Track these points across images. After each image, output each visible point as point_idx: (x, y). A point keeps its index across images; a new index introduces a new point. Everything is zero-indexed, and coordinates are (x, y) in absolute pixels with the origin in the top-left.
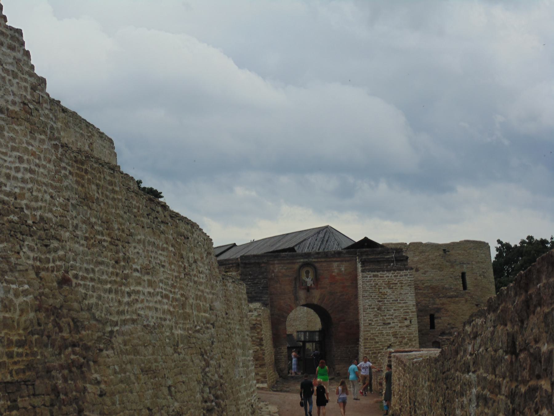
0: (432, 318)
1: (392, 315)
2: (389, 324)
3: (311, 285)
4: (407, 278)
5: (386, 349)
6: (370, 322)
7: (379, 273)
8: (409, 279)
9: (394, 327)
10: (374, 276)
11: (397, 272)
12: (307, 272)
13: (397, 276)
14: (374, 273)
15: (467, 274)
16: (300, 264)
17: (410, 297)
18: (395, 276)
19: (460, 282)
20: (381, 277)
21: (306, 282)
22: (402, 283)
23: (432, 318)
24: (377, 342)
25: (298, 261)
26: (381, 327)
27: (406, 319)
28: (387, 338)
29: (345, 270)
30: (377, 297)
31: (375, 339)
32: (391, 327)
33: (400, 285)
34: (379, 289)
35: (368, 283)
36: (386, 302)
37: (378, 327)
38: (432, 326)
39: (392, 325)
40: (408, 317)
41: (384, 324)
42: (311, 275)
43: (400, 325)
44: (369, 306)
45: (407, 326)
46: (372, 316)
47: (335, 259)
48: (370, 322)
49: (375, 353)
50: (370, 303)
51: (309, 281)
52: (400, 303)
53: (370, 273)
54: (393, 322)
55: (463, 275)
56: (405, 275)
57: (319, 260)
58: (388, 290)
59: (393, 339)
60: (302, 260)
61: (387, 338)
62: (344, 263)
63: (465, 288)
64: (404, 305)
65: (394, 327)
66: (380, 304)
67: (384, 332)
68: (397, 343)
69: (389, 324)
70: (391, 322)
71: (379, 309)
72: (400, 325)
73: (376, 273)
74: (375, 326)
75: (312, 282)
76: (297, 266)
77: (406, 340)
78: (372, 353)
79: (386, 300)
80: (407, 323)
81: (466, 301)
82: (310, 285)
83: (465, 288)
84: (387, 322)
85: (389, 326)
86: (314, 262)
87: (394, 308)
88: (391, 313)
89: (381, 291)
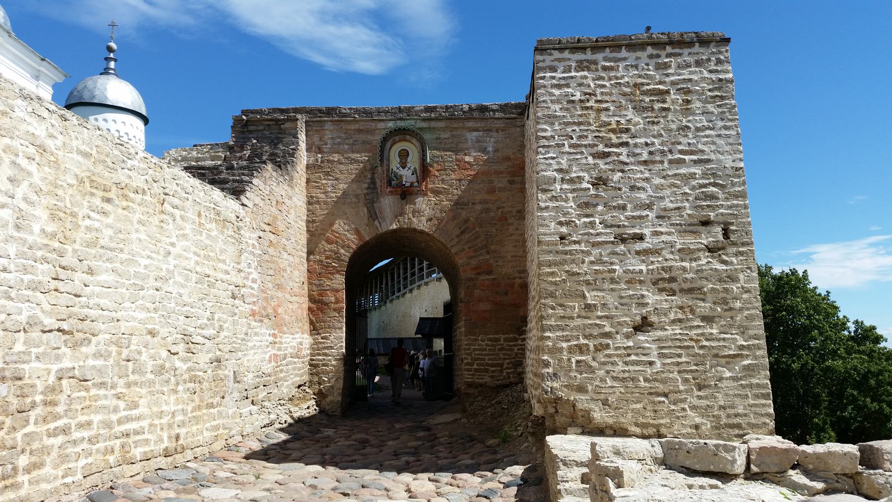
1: (649, 207)
2: (641, 238)
3: (412, 184)
4: (706, 74)
5: (628, 336)
6: (564, 230)
8: (714, 77)
9: (657, 252)
10: (581, 66)
11: (669, 49)
12: (404, 155)
13: (667, 66)
14: (580, 56)
16: (384, 132)
17: (720, 142)
20: (605, 69)
21: (399, 178)
22: (688, 92)
25: (381, 125)
26: (605, 251)
27: (706, 223)
29: (496, 151)
30: (589, 141)
31: (584, 297)
32: (646, 252)
33: (680, 98)
34: (599, 111)
35: (557, 92)
36: (623, 158)
37: (596, 251)
42: (414, 161)
44: (560, 171)
45: (711, 250)
47: (470, 124)
48: (564, 230)
49: (581, 349)
50: (564, 162)
51: (407, 175)
52: (680, 162)
53: (566, 55)
54: (656, 234)
56: (698, 63)
57: (433, 124)
58: (630, 114)
59: (652, 298)
60: (391, 124)
62: (494, 134)
64: (697, 170)
65: (657, 252)
68: (672, 316)
70: (647, 232)
71: (600, 182)
73: (589, 55)
74: (583, 247)
75: (413, 179)
78: (570, 350)
79: (624, 150)
82: (408, 184)
84: (631, 231)
85: (639, 246)
86: (420, 129)
87: (657, 181)
89: (604, 118)
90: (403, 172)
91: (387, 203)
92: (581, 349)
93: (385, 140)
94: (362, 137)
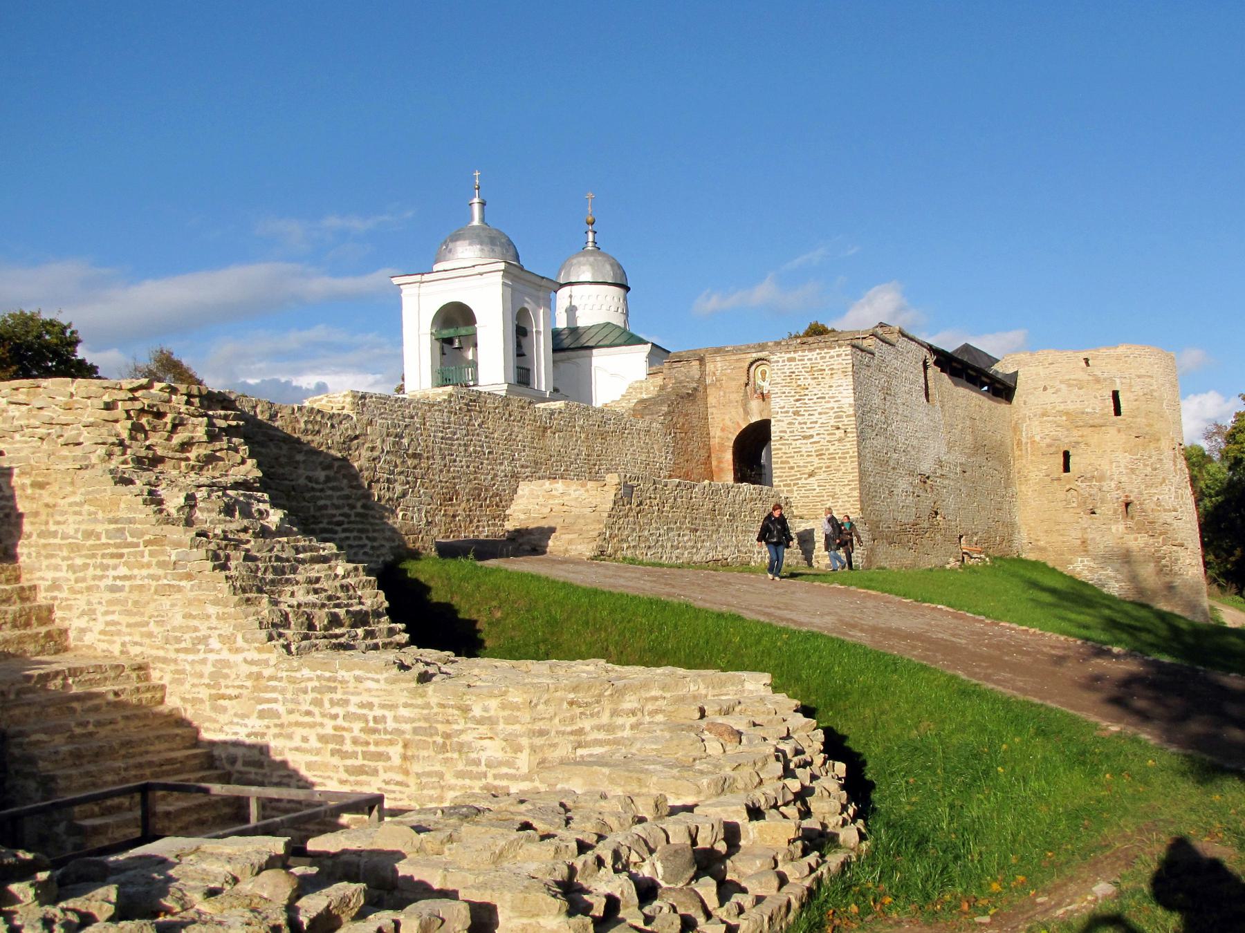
0: (1066, 455)
2: (812, 436)
7: (796, 355)
10: (790, 360)
14: (788, 355)
15: (1120, 394)
18: (822, 358)
19: (1110, 403)
23: (1066, 455)
24: (792, 468)
28: (809, 459)
38: (1066, 468)
39: (816, 439)
40: (840, 425)
41: (805, 437)
43: (828, 438)
45: (840, 440)
46: (784, 425)
49: (789, 485)
55: (1115, 395)
58: (810, 381)
59: (816, 460)
61: (809, 459)
63: (1117, 412)
64: (836, 405)
66: (798, 404)
67: (804, 450)
69: (812, 436)
72: (828, 438)
73: (792, 355)
76: (747, 365)
77: (838, 462)
80: (839, 433)
81: (1119, 431)
83: (1117, 412)
88: (814, 418)
90: (763, 384)
91: (755, 404)
92: (789, 485)
93: (752, 364)
94: (738, 365)
